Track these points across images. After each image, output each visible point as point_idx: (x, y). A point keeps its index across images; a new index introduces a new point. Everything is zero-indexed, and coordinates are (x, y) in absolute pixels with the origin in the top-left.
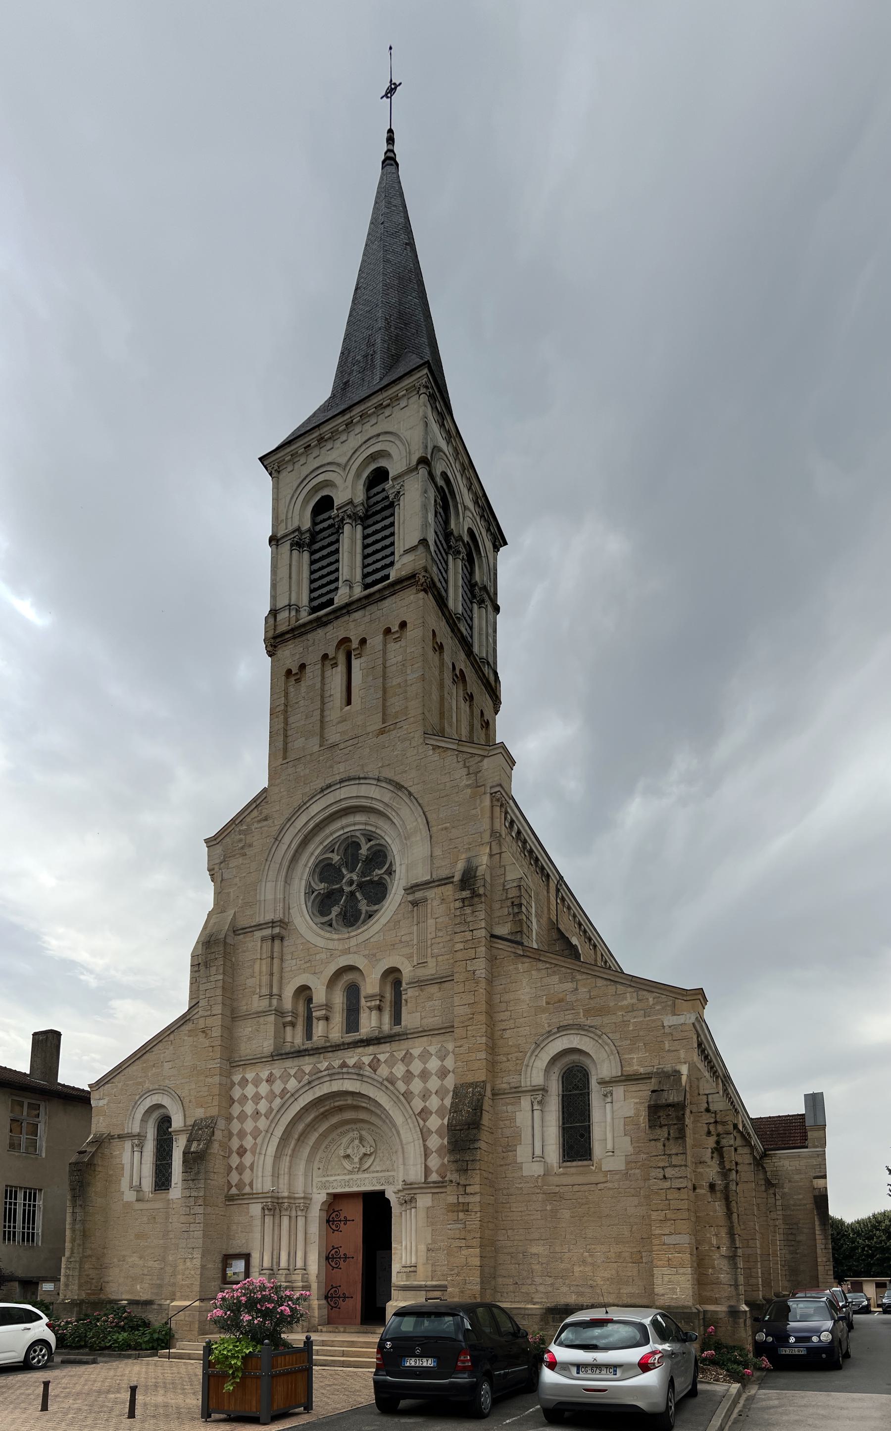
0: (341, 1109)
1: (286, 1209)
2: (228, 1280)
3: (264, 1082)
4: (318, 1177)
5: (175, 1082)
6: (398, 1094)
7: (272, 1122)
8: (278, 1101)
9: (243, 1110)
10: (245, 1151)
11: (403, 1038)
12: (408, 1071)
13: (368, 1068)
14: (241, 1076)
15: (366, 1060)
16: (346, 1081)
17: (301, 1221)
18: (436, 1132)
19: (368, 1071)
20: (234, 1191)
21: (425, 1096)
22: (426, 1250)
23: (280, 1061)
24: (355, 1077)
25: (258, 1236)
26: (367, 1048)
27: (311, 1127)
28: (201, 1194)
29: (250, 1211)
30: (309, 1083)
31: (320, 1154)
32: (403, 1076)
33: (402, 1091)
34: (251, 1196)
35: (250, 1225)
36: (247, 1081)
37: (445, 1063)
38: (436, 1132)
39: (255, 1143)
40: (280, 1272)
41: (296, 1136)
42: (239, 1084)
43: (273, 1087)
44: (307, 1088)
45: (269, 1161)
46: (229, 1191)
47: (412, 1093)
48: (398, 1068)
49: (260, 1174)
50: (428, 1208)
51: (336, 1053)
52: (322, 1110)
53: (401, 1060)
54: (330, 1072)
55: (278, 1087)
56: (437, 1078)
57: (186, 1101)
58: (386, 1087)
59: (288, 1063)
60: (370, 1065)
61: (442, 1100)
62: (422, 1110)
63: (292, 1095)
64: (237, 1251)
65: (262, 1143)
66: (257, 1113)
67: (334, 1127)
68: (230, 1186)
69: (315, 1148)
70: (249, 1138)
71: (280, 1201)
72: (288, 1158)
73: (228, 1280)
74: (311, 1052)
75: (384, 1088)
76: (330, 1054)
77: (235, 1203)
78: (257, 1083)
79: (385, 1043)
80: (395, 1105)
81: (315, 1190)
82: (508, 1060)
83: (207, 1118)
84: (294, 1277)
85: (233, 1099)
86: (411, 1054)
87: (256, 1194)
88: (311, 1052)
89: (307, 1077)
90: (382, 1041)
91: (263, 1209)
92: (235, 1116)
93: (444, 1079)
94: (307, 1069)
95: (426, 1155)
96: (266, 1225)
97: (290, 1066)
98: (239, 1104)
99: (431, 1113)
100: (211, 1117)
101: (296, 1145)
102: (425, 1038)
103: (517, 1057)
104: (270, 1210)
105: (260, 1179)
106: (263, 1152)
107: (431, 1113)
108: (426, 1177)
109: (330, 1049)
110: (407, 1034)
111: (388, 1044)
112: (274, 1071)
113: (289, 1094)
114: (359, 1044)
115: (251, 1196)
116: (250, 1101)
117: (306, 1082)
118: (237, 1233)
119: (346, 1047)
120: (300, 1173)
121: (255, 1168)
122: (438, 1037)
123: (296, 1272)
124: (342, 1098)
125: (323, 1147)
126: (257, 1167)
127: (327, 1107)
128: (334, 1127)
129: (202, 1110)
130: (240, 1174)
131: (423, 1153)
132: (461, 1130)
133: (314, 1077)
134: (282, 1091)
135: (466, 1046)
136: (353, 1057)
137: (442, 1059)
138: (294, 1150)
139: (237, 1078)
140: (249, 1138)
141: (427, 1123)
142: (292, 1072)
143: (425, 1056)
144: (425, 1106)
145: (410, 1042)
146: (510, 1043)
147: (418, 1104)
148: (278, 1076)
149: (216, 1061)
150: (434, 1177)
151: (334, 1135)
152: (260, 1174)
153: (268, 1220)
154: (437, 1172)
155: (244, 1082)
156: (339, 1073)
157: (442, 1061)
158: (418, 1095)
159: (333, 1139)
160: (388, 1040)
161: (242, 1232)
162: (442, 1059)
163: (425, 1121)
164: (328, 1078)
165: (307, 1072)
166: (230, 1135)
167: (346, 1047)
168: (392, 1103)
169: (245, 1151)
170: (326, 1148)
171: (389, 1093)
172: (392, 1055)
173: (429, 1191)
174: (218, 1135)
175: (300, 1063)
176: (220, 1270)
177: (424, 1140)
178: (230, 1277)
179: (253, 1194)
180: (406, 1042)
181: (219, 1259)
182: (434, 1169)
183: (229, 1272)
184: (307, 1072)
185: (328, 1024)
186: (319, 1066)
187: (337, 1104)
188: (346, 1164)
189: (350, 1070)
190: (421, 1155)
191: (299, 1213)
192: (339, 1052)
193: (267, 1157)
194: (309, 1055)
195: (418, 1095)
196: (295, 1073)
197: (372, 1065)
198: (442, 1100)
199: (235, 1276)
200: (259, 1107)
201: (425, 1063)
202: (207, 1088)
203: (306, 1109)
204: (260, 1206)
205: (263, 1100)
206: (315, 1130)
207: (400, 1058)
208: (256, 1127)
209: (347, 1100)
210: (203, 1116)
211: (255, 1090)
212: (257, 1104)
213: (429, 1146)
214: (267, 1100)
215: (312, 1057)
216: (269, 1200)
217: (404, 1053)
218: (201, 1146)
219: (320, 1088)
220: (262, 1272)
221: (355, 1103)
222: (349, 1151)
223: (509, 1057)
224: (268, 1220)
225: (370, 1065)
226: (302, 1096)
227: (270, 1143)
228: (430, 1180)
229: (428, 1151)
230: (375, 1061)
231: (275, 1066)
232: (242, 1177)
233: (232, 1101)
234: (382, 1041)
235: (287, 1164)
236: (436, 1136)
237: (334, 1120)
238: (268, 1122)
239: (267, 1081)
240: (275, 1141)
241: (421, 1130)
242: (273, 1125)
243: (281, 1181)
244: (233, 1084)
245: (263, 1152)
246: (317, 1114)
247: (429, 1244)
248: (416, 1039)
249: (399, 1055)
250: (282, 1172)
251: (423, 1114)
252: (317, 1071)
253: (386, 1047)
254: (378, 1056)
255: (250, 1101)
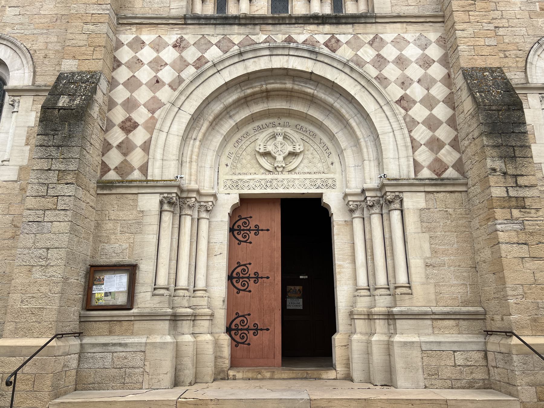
0: (267, 95)
1: (190, 207)
2: (94, 303)
3: (170, 47)
4: (227, 174)
5: (23, 31)
6: (369, 78)
7: (181, 93)
8: (191, 71)
9: (134, 76)
10: (135, 125)
11: (371, 21)
12: (378, 55)
13: (324, 47)
14: (134, 36)
15: (322, 39)
16: (291, 57)
17: (204, 224)
18: (423, 123)
19: (326, 51)
20: (112, 175)
21: (404, 83)
22: (423, 266)
23: (197, 27)
24: (306, 55)
25: (153, 239)
26: (321, 27)
27: (227, 112)
28: (72, 167)
29: (140, 204)
30: (241, 54)
31: (229, 148)
32: (372, 60)
33: (374, 76)
34: (145, 184)
35: (139, 223)
36: (143, 43)
37: (427, 52)
38: (423, 123)
39: (152, 118)
40: (181, 293)
41: (211, 118)
42: (130, 45)
43: (183, 54)
44: (236, 60)
45: (175, 141)
46: (102, 175)
47: (386, 78)
48: (366, 52)
49: (159, 156)
50: (421, 210)
51: (278, 27)
52: (249, 91)
53: (369, 43)
54: (272, 45)
55: (191, 54)
56: (418, 67)
57: (39, 56)
58: (352, 69)
59: (208, 30)
60: (326, 44)
61: (428, 89)
62: (402, 98)
63: (215, 65)
64: (115, 260)
65: (165, 119)
66: (158, 82)
67: (252, 118)
68: (105, 168)
69: (226, 139)
70: (143, 110)
71: (184, 195)
72: (197, 143)
73: (94, 303)
74: (243, 21)
75: (347, 70)
76: (270, 27)
77: (114, 191)
78: (158, 46)
79: (346, 23)
80: (363, 90)
81: (222, 189)
82: (506, 57)
83: (80, 73)
84: (195, 301)
85: (118, 61)
86: (382, 39)
87: (153, 181)
88: (243, 21)
89: (236, 47)
90: (343, 21)
91: (161, 203)
92: (121, 82)
93: (427, 68)
94: (237, 39)
95: (413, 147)
96: (163, 225)
97: (211, 33)
98: (128, 67)
99: (415, 102)
100: (89, 72)
101: (208, 129)
102: (399, 25)
103: (515, 55)
104: (170, 203)
105: (158, 164)
106: (166, 129)
107: (415, 102)
108: (416, 173)
109: (270, 21)
110: (376, 17)
111: (350, 26)
112: (185, 37)
113: (210, 64)
114: (312, 21)
115: (145, 184)
116: (146, 67)
117: (237, 52)
118: (114, 233)
119: (293, 21)
120: (208, 165)
121: (152, 147)
122: (415, 25)
123: (199, 293)
124: (278, 81)
125: (235, 139)
126: (156, 146)
127: (257, 89)
128: (252, 118)
129: (76, 62)
130: (125, 154)
131: (409, 144)
132: (498, 111)
133: (248, 48)
134: (199, 59)
135: (470, 31)
136: (302, 33)
137: (424, 47)
138: (204, 135)
139: (127, 37)
140: (143, 110)
141: (410, 113)
142: (214, 40)
143: (399, 42)
144: (406, 94)
145: (380, 27)
146: (507, 41)
147: (395, 92)
148: (192, 43)
149: (104, 7)
150: (426, 173)
151: (249, 128)
152: (159, 156)
153: (167, 217)
154: (429, 167)
155: (137, 44)
156: (284, 48)
157: (424, 49)
158: (395, 82)
159: (247, 133)
160: (350, 21)
161: (122, 232)
162: (424, 47)
163: (406, 110)
164: (267, 52)
165: (236, 43)
166: (111, 104)
167: (293, 21)
168: (359, 87)
169: (135, 125)
170: (237, 142)
171: (354, 75)
172: (356, 36)
173: (422, 189)
174: (99, 97)
175: (226, 32)
176: (81, 289)
177: (410, 132)
178: (98, 299)
179: (147, 181)
180: (374, 24)
181: (82, 270)
182: (425, 164)
183: (98, 292)
184: (236, 43)
185: (250, 5)
186: (253, 37)
187: (270, 86)
188: (263, 161)
189: (301, 46)
190: (406, 147)
191: (204, 215)
192: (283, 27)
193: (170, 136)
194: (239, 24)
195: (395, 82)
196: (219, 42)
197: (329, 44)
198: (428, 89)
199: (109, 298)
200: (160, 75)
201: (401, 50)
202: (85, 37)
203: (228, 87)
204: (156, 199)
205: (168, 67)
206: (231, 117)
207: (367, 42)
208: (154, 98)
209: (285, 84)
210: (74, 69)
211: (155, 55)
212: (157, 71)
213: (415, 137)
214: (173, 67)
215: (243, 27)
216: (175, 190)
217: (372, 37)
218: (77, 102)
219: (255, 62)
220: (157, 292)
221: (296, 87)
222: (270, 148)
223: (507, 53)
224: (167, 217)
225: (326, 44)
226: (228, 69)
227: (176, 119)
228: (419, 177)
229: (415, 144)
230: (333, 41)
231: (188, 31)
232: (128, 158)
233: (117, 64)
234: (343, 21)
235: (196, 150)
236: (424, 128)
237: (257, 108)
238: (176, 93)
239: (175, 46)
240: (184, 118)
241: (405, 119)
242: (183, 98)
243: (186, 170)
244: (119, 44)
245: (166, 129)
246: (242, 95)
247: (428, 258)
248: (387, 25)
249: (365, 38)
250: (188, 160)
251: (403, 102)
252: (251, 42)
253: (348, 28)
254: (338, 36)
255: (146, 67)
